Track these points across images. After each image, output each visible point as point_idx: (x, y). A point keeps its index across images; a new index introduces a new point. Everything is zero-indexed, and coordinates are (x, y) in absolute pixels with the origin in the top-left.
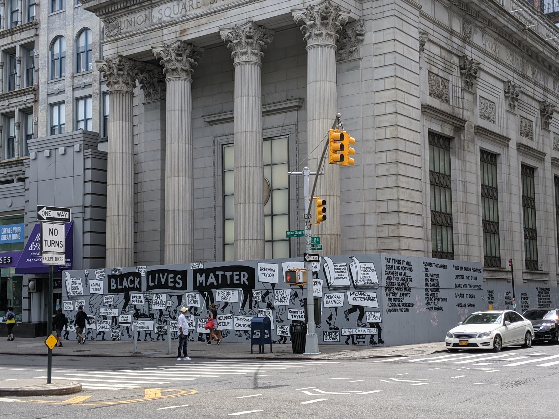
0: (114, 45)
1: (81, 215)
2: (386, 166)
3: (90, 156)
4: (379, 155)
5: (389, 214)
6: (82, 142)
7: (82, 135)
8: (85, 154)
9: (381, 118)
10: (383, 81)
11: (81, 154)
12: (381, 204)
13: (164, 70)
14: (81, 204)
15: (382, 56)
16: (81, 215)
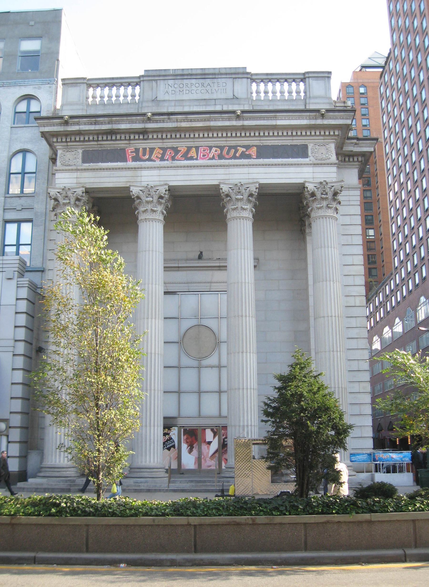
0: (75, 175)
1: (11, 349)
2: (356, 330)
3: (27, 285)
4: (349, 319)
5: (359, 372)
6: (17, 269)
7: (18, 262)
8: (19, 283)
9: (351, 288)
10: (351, 257)
11: (14, 283)
12: (352, 362)
13: (309, 210)
14: (12, 337)
15: (350, 237)
16: (11, 349)
